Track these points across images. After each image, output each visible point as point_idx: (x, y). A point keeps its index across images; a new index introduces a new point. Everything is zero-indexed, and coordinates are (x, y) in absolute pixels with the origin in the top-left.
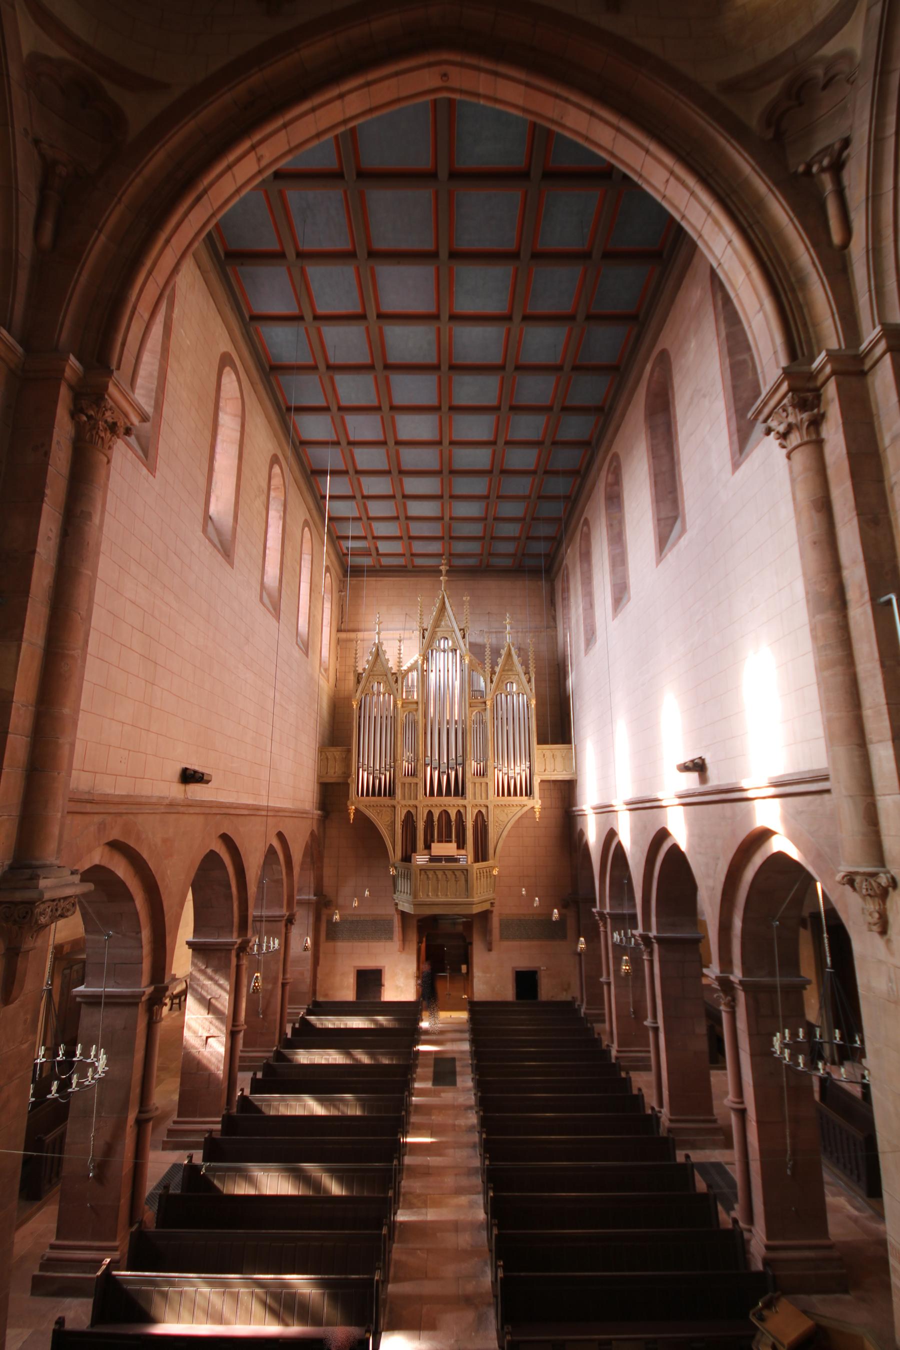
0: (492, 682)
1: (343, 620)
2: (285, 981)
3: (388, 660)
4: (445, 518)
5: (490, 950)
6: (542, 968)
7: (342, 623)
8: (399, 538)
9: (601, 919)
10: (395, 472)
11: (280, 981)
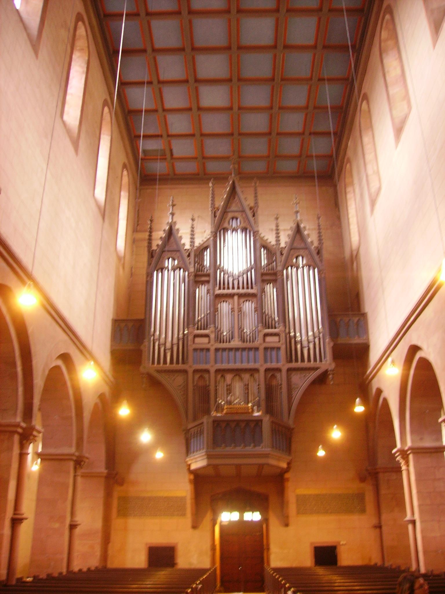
0: (282, 254)
1: (139, 222)
2: (74, 523)
3: (181, 238)
4: (234, 108)
5: (287, 525)
6: (342, 543)
7: (138, 225)
8: (193, 135)
9: (403, 458)
10: (188, 49)
11: (68, 522)
